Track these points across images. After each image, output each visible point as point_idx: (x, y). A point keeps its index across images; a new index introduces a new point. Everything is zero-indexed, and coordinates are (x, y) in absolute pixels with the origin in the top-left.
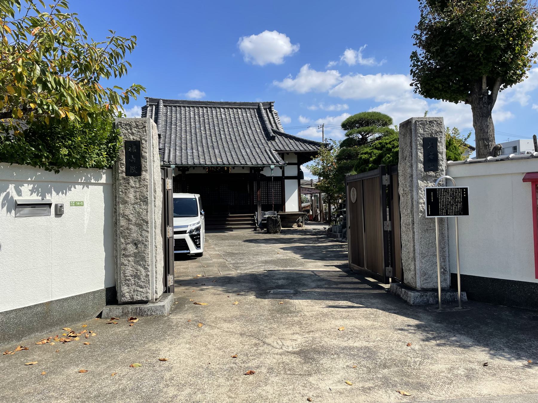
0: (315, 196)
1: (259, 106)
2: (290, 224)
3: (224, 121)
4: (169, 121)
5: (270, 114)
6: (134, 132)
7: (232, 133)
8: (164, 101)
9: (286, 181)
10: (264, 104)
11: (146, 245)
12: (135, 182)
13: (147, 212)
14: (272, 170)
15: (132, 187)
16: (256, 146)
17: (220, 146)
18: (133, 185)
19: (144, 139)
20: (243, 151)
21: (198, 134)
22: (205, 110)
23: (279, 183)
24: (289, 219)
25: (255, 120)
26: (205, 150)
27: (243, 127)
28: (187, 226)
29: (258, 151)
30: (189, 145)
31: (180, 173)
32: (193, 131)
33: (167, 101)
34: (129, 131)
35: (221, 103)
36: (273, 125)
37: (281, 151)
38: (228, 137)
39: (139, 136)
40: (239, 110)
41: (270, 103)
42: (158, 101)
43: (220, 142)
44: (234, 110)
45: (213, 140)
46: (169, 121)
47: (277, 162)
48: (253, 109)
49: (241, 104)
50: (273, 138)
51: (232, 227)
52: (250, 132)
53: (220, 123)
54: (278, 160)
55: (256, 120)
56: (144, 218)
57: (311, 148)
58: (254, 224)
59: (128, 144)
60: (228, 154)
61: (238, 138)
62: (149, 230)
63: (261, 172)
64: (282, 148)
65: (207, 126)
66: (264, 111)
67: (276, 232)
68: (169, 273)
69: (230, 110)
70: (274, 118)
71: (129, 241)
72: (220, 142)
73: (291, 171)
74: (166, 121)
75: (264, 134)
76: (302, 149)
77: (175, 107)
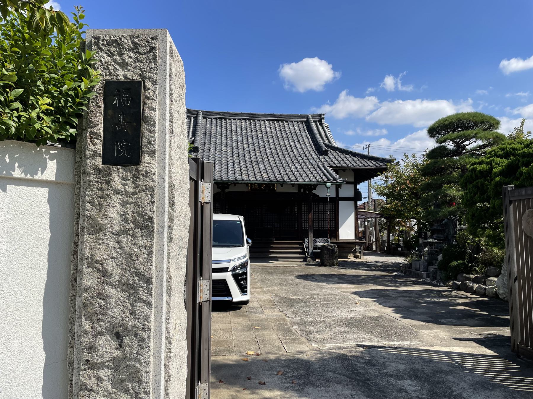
0: (368, 221)
1: (308, 119)
2: (344, 254)
3: (269, 135)
4: (208, 133)
5: (320, 128)
6: (128, 60)
7: (278, 147)
8: (204, 113)
9: (340, 202)
10: (313, 116)
11: (142, 340)
12: (124, 179)
13: (150, 254)
14: (328, 188)
15: (117, 192)
16: (307, 161)
17: (266, 161)
18: (120, 187)
19: (150, 78)
20: (292, 167)
21: (240, 148)
24: (346, 247)
25: (303, 134)
26: (248, 165)
27: (291, 140)
28: (229, 261)
29: (310, 166)
30: (230, 159)
31: (219, 190)
32: (234, 144)
33: (206, 112)
34: (117, 57)
35: (266, 116)
36: (325, 138)
37: (337, 167)
38: (274, 151)
39: (138, 71)
40: (286, 123)
41: (321, 115)
42: (197, 113)
43: (265, 157)
44: (280, 122)
45: (258, 154)
46: (208, 133)
47: (335, 179)
48: (301, 122)
49: (287, 116)
50: (326, 153)
51: (278, 255)
52: (298, 146)
53: (265, 136)
54: (336, 177)
55: (305, 133)
56: (141, 269)
57: (372, 164)
58: (304, 253)
59: (112, 88)
60: (275, 170)
61: (285, 152)
62: (153, 300)
63: (314, 192)
64: (338, 164)
65: (250, 140)
66: (313, 124)
67: (332, 265)
68: (199, 379)
69: (275, 122)
70: (325, 132)
71: (102, 327)
72: (265, 157)
73: (347, 191)
74: (205, 134)
75: (314, 149)
76: (361, 165)
77: (215, 119)
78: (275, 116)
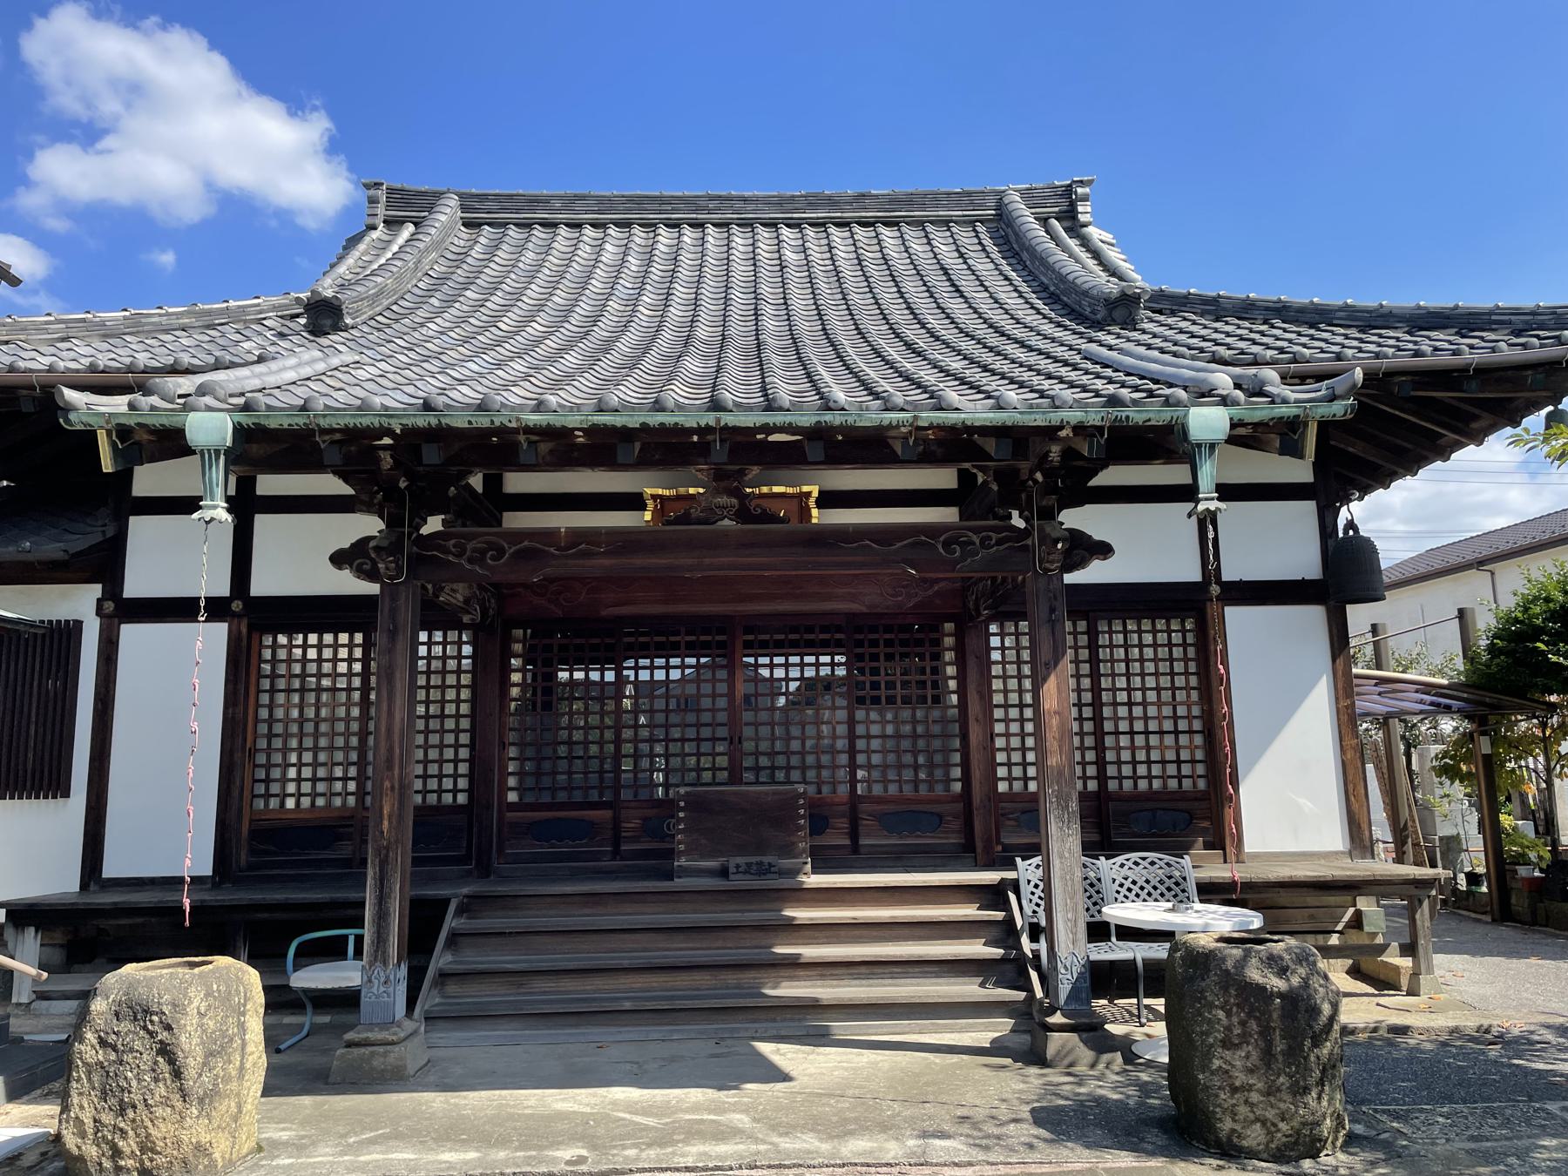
1: (1001, 207)
3: (795, 277)
22: (689, 236)
23: (1179, 631)
25: (983, 267)
33: (483, 198)
41: (1068, 190)
48: (971, 223)
78: (832, 202)
